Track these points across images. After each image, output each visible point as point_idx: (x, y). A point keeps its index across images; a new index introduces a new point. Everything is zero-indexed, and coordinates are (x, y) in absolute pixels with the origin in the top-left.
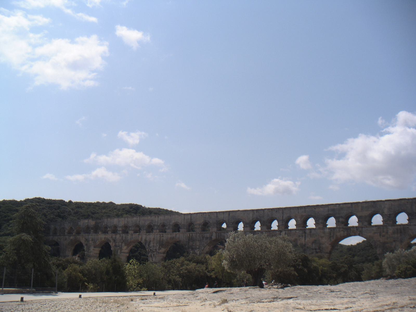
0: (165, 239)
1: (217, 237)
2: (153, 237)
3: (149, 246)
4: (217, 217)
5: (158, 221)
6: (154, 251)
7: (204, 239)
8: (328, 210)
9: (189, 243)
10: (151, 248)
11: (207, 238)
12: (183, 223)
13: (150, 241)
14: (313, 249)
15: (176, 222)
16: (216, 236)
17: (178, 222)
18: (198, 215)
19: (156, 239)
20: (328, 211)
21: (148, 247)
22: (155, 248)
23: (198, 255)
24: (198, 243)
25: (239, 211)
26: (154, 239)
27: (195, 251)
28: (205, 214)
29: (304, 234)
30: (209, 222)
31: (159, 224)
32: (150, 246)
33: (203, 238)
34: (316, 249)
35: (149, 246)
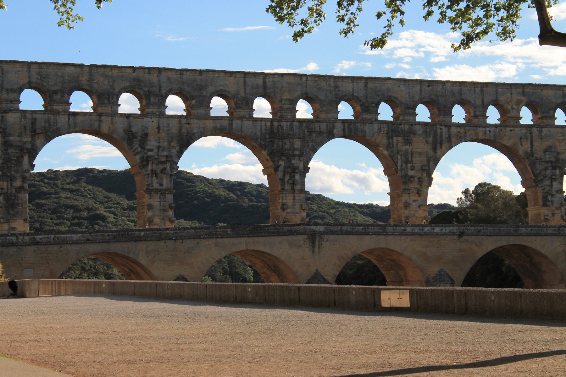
0: (195, 131)
1: (347, 132)
2: (155, 124)
3: (143, 148)
4: (336, 87)
5: (159, 81)
6: (163, 159)
7: (314, 135)
8: (563, 95)
9: (272, 143)
10: (150, 153)
11: (320, 133)
12: (242, 94)
13: (146, 135)
14: (547, 162)
15: (221, 90)
16: (344, 130)
17: (228, 92)
18: (287, 79)
19: (165, 129)
20: (563, 98)
21: (139, 149)
22: (166, 153)
23: (302, 170)
24: (297, 144)
25: (389, 79)
26: (159, 128)
27: (291, 161)
28: (304, 79)
29: (529, 134)
30: (317, 97)
31: (163, 92)
32: (148, 147)
33: (310, 132)
34: (551, 162)
35: (143, 148)
